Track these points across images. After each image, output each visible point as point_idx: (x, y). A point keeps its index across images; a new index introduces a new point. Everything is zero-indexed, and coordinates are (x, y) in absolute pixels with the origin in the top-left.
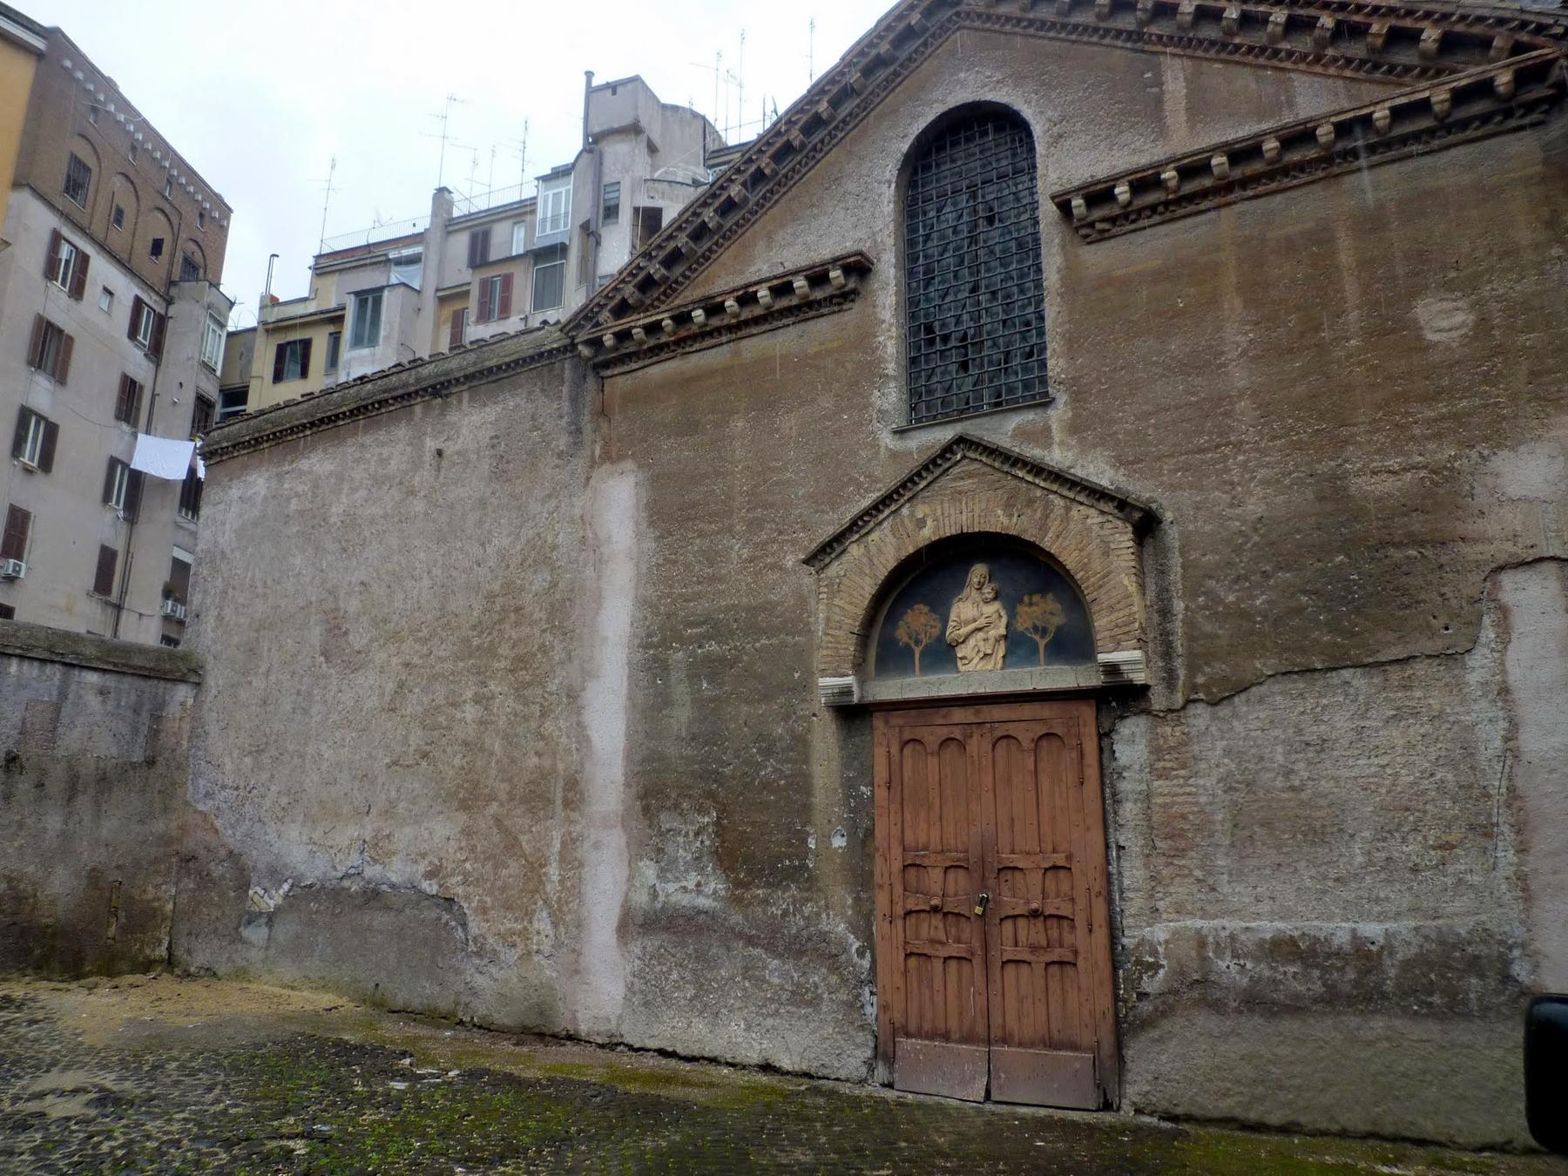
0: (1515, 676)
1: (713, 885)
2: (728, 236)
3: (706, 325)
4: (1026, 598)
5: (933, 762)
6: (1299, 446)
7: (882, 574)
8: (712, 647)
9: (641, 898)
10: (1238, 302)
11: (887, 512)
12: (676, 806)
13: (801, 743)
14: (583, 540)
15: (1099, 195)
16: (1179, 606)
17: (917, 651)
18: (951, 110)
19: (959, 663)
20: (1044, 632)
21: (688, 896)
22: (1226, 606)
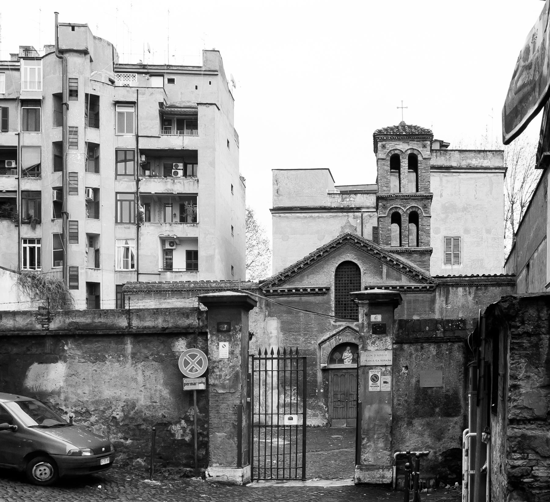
5: (339, 378)
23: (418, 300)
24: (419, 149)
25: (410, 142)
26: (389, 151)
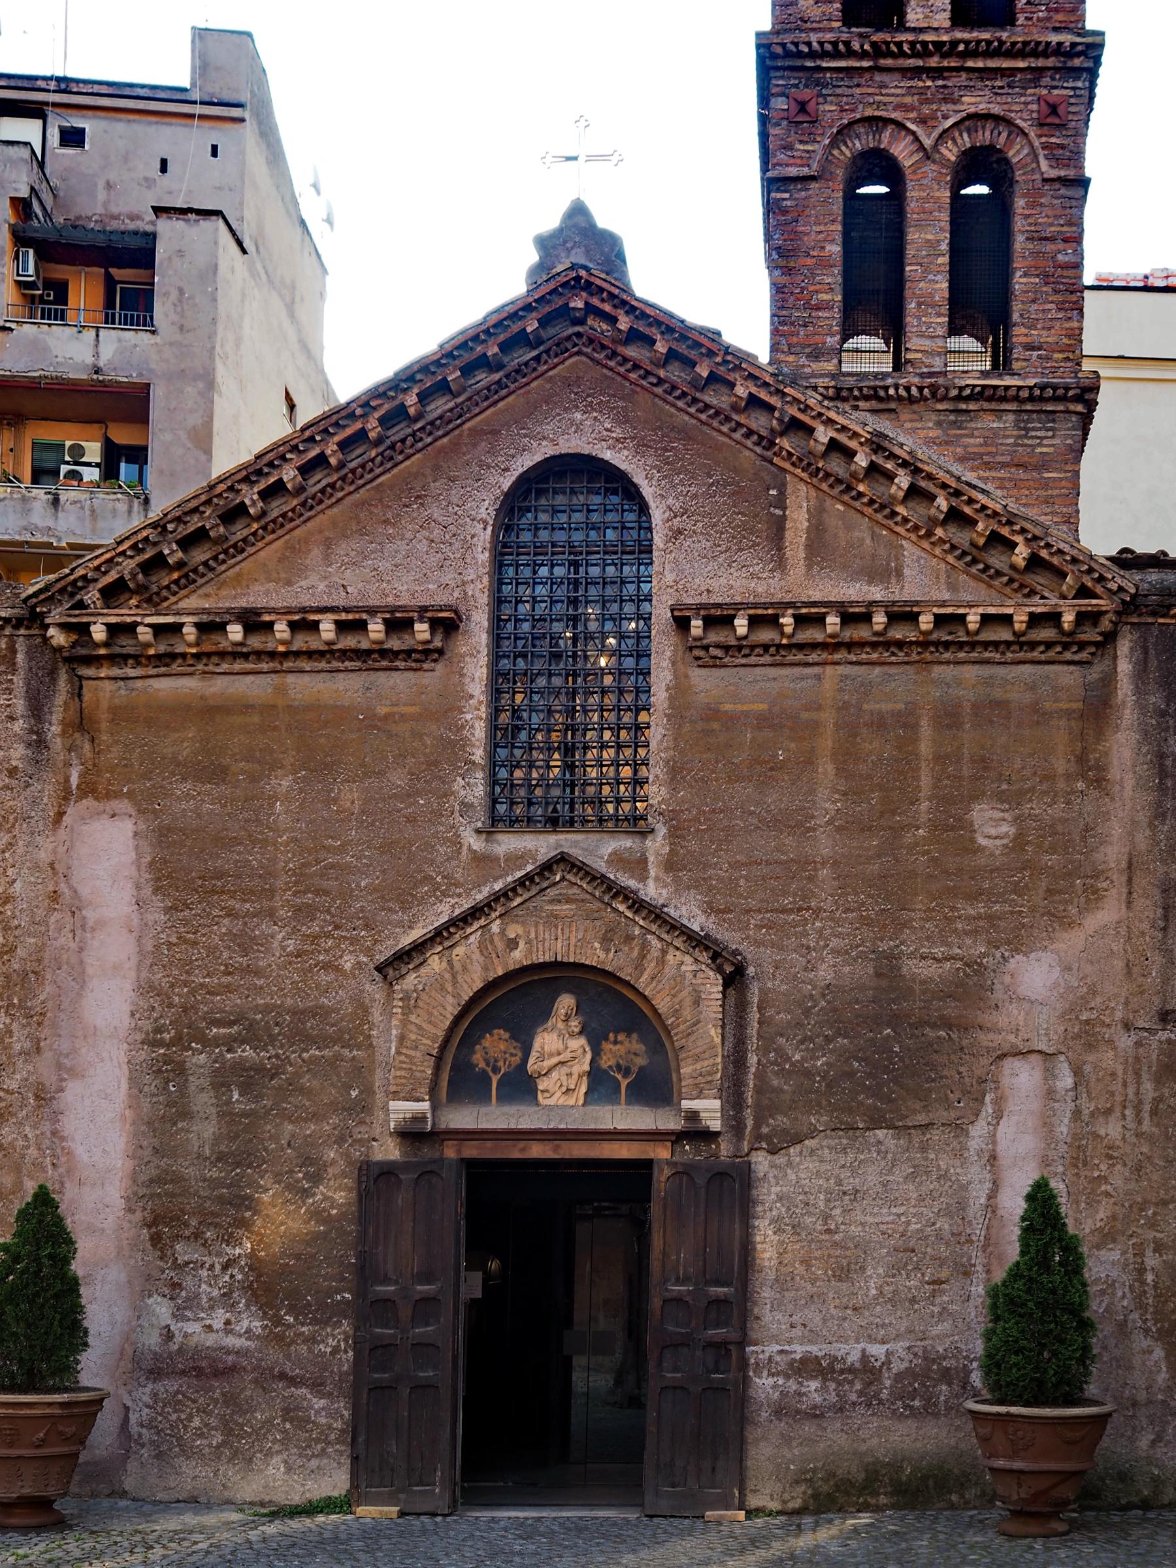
0: (1004, 1147)
1: (245, 1324)
3: (241, 644)
6: (866, 922)
9: (152, 1340)
10: (830, 768)
12: (197, 1235)
14: (55, 896)
15: (718, 619)
16: (753, 1059)
18: (561, 456)
19: (540, 1096)
20: (626, 1072)
22: (793, 1064)
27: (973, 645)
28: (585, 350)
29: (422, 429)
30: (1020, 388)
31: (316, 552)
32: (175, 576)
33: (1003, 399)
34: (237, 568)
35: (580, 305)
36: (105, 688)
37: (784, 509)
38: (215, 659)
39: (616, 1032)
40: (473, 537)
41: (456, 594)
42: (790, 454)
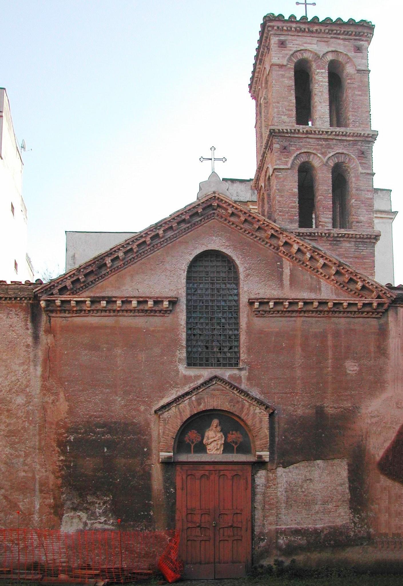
1: (111, 521)
2: (115, 270)
4: (231, 432)
7: (185, 419)
8: (108, 436)
10: (300, 349)
11: (187, 398)
12: (94, 494)
13: (147, 476)
15: (263, 303)
17: (192, 446)
19: (208, 451)
20: (236, 443)
21: (101, 525)
23: (353, 330)
24: (349, 54)
25: (332, 40)
26: (291, 52)
27: (344, 312)
28: (216, 218)
29: (163, 241)
30: (356, 235)
31: (128, 279)
32: (82, 285)
33: (351, 238)
34: (101, 283)
35: (216, 205)
36: (58, 321)
37: (282, 268)
38: (95, 312)
39: (232, 431)
40: (180, 274)
41: (175, 293)
42: (284, 252)
